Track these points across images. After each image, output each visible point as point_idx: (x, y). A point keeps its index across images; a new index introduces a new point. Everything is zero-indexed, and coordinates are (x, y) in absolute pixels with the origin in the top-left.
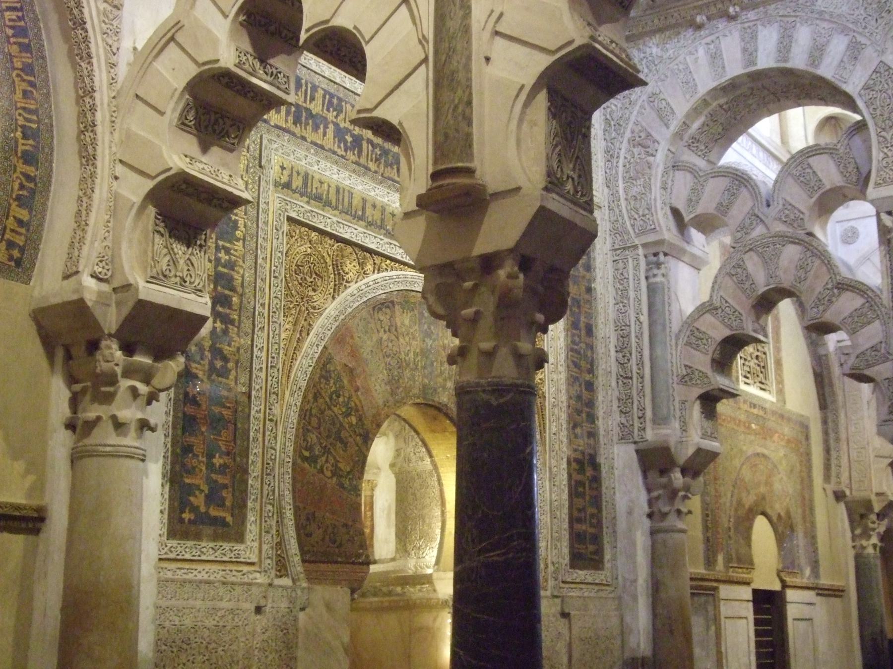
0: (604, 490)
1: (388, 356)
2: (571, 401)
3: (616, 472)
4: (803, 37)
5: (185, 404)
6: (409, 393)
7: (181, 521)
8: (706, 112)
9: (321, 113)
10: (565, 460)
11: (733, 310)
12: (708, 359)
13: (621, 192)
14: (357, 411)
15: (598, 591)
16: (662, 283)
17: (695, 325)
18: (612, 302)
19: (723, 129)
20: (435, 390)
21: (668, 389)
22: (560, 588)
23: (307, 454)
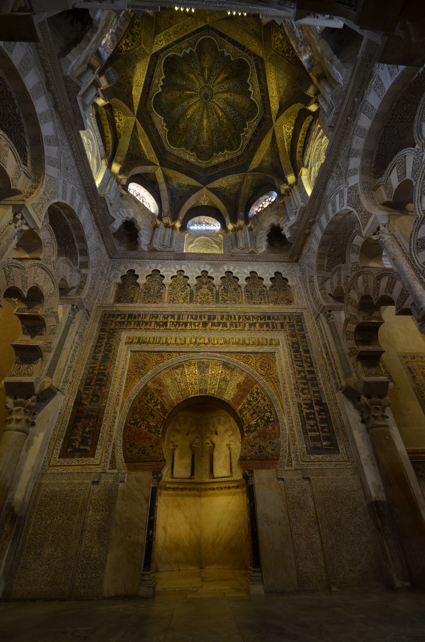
0: (331, 415)
1: (180, 383)
2: (298, 381)
3: (339, 405)
4: (330, 207)
6: (191, 393)
8: (326, 257)
12: (353, 341)
14: (161, 403)
15: (336, 465)
16: (332, 322)
17: (347, 330)
18: (320, 337)
19: (342, 258)
20: (207, 390)
22: (301, 465)
23: (133, 422)
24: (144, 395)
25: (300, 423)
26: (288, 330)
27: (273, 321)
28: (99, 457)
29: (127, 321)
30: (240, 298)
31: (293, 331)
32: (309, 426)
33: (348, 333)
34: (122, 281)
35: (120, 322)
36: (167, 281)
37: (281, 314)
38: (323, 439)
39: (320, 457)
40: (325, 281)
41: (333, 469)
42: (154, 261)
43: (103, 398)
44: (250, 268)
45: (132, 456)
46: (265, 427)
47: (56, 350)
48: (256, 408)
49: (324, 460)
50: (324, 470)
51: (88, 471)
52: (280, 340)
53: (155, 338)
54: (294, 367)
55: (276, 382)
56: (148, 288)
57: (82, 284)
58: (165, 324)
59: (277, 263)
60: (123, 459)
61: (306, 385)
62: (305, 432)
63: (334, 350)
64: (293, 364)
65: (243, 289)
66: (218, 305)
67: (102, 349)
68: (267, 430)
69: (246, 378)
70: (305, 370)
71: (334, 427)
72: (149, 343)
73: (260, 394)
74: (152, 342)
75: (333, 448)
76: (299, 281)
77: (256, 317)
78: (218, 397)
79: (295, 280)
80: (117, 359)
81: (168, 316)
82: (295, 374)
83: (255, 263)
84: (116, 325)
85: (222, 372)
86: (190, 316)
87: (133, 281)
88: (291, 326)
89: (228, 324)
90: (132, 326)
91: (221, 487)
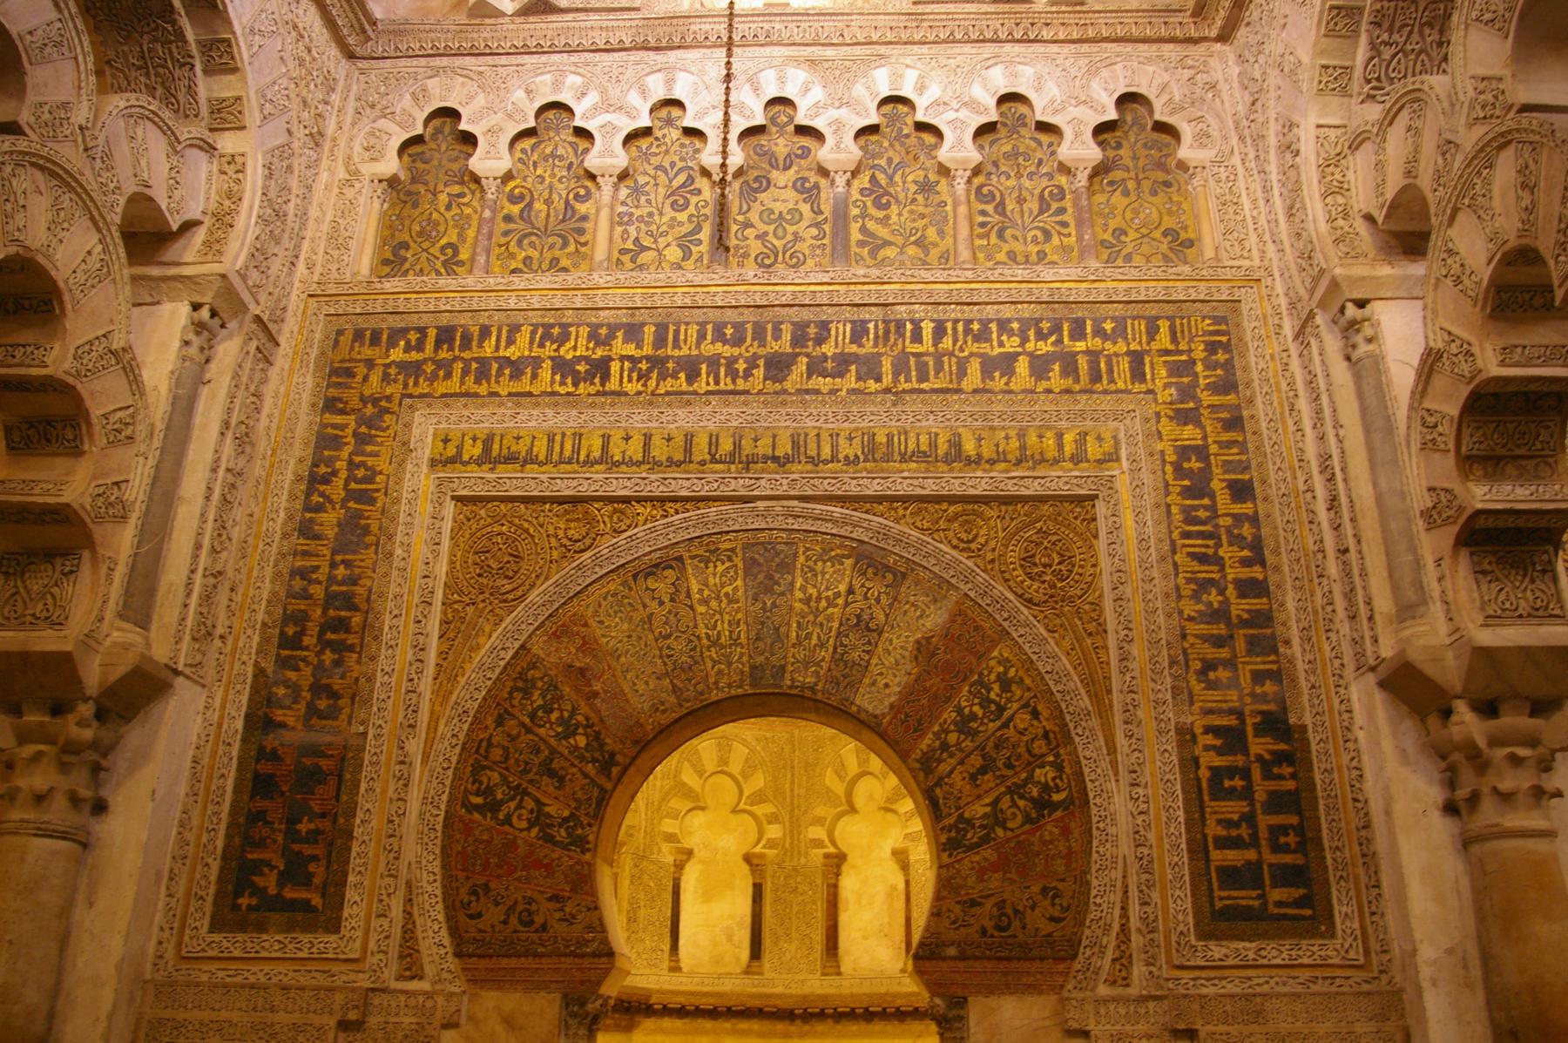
0: (1318, 778)
1: (668, 637)
2: (1191, 628)
3: (1361, 735)
5: (258, 761)
6: (716, 683)
7: (236, 907)
8: (1364, 27)
9: (526, 353)
10: (1172, 733)
11: (1458, 342)
12: (1450, 461)
13: (1284, 236)
15: (1314, 980)
16: (1370, 355)
17: (1427, 405)
18: (1307, 424)
20: (783, 668)
21: (1413, 549)
22: (1168, 980)
23: (479, 800)
24: (518, 689)
25: (1181, 813)
26: (1166, 386)
27: (1095, 343)
28: (359, 933)
29: (434, 361)
30: (949, 229)
31: (1187, 393)
32: (1219, 822)
33: (1431, 420)
34: (409, 169)
35: (402, 366)
36: (607, 156)
37: (1136, 310)
38: (1272, 877)
39: (1248, 949)
40: (1355, 145)
41: (1298, 996)
42: (544, 58)
43: (353, 699)
44: (1001, 81)
45: (481, 931)
46: (1027, 827)
47: (148, 509)
48: (997, 747)
49: (1265, 962)
50: (1258, 1000)
51: (323, 981)
52: (1121, 435)
53: (558, 438)
54: (1175, 565)
55: (1090, 634)
56: (522, 197)
57: (227, 203)
58: (600, 368)
59: (1129, 48)
60: (447, 941)
61: (1221, 646)
62: (1199, 849)
63: (1364, 491)
64: (1174, 552)
65: (960, 186)
66: (840, 271)
67: (337, 490)
68: (1035, 839)
69: (959, 614)
70: (1224, 576)
71: (1324, 826)
72: (530, 459)
73: (1014, 687)
74: (542, 458)
75: (1308, 912)
76: (1234, 141)
77: (1015, 325)
78: (833, 701)
79: (1215, 134)
80: (399, 538)
81: (613, 329)
82: (1180, 597)
83: (1018, 48)
84: (386, 378)
85: (851, 591)
86: (710, 327)
87: (455, 167)
88: (1176, 370)
89: (887, 365)
90: (454, 385)
91: (866, 1009)
